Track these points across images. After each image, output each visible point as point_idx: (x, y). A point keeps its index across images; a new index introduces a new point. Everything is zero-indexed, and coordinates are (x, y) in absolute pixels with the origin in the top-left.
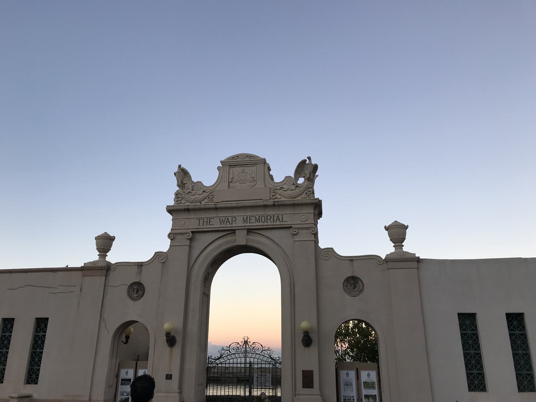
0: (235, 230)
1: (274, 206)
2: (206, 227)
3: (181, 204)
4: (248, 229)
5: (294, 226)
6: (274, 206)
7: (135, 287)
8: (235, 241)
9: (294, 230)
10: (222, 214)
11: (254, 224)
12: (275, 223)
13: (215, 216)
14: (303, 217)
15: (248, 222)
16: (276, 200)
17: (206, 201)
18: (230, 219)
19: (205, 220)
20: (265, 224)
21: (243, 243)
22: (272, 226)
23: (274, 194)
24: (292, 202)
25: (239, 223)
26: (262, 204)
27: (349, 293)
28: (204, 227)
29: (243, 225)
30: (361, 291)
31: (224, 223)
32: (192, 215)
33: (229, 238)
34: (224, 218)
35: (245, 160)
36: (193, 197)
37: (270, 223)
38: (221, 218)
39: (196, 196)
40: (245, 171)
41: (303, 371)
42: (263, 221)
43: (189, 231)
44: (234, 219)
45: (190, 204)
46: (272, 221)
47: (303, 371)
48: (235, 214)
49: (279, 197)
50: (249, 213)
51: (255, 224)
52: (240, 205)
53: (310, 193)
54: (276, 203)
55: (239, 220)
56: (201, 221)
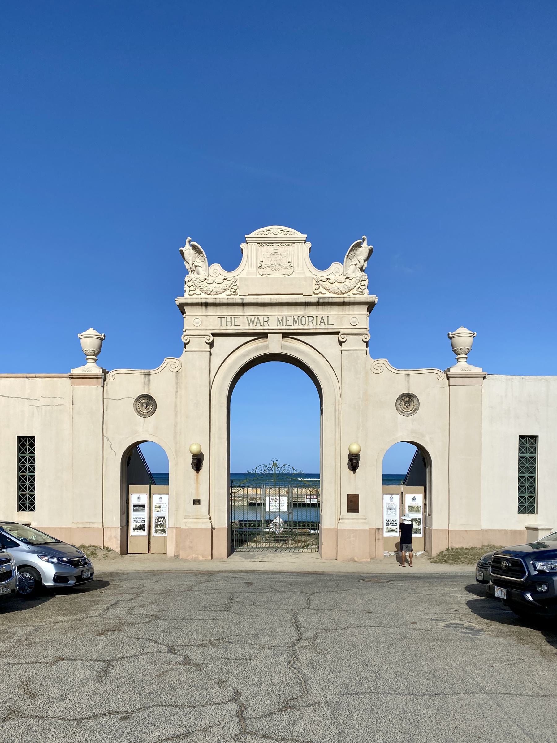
0: (267, 334)
1: (318, 304)
2: (230, 329)
3: (195, 296)
4: (283, 334)
5: (342, 331)
6: (318, 304)
7: (143, 401)
8: (267, 347)
9: (343, 336)
10: (250, 311)
11: (293, 328)
12: (318, 327)
13: (241, 314)
14: (354, 319)
15: (285, 324)
16: (320, 295)
17: (228, 292)
18: (261, 318)
19: (229, 319)
20: (306, 327)
21: (277, 350)
22: (314, 331)
23: (317, 287)
24: (341, 300)
25: (273, 325)
26: (303, 300)
27: (402, 413)
28: (228, 328)
29: (278, 327)
30: (416, 410)
31: (253, 323)
32: (211, 311)
33: (260, 343)
34: (253, 318)
35: (278, 236)
36: (211, 287)
37: (311, 327)
38: (249, 317)
39: (214, 285)
40: (279, 252)
41: (348, 495)
42: (303, 323)
43: (209, 333)
44: (266, 319)
45: (207, 296)
46: (315, 324)
47: (348, 495)
48: (267, 311)
49: (324, 291)
50: (285, 311)
51: (293, 327)
52: (274, 301)
53: (363, 287)
54: (321, 301)
55: (272, 320)
56: (224, 320)
